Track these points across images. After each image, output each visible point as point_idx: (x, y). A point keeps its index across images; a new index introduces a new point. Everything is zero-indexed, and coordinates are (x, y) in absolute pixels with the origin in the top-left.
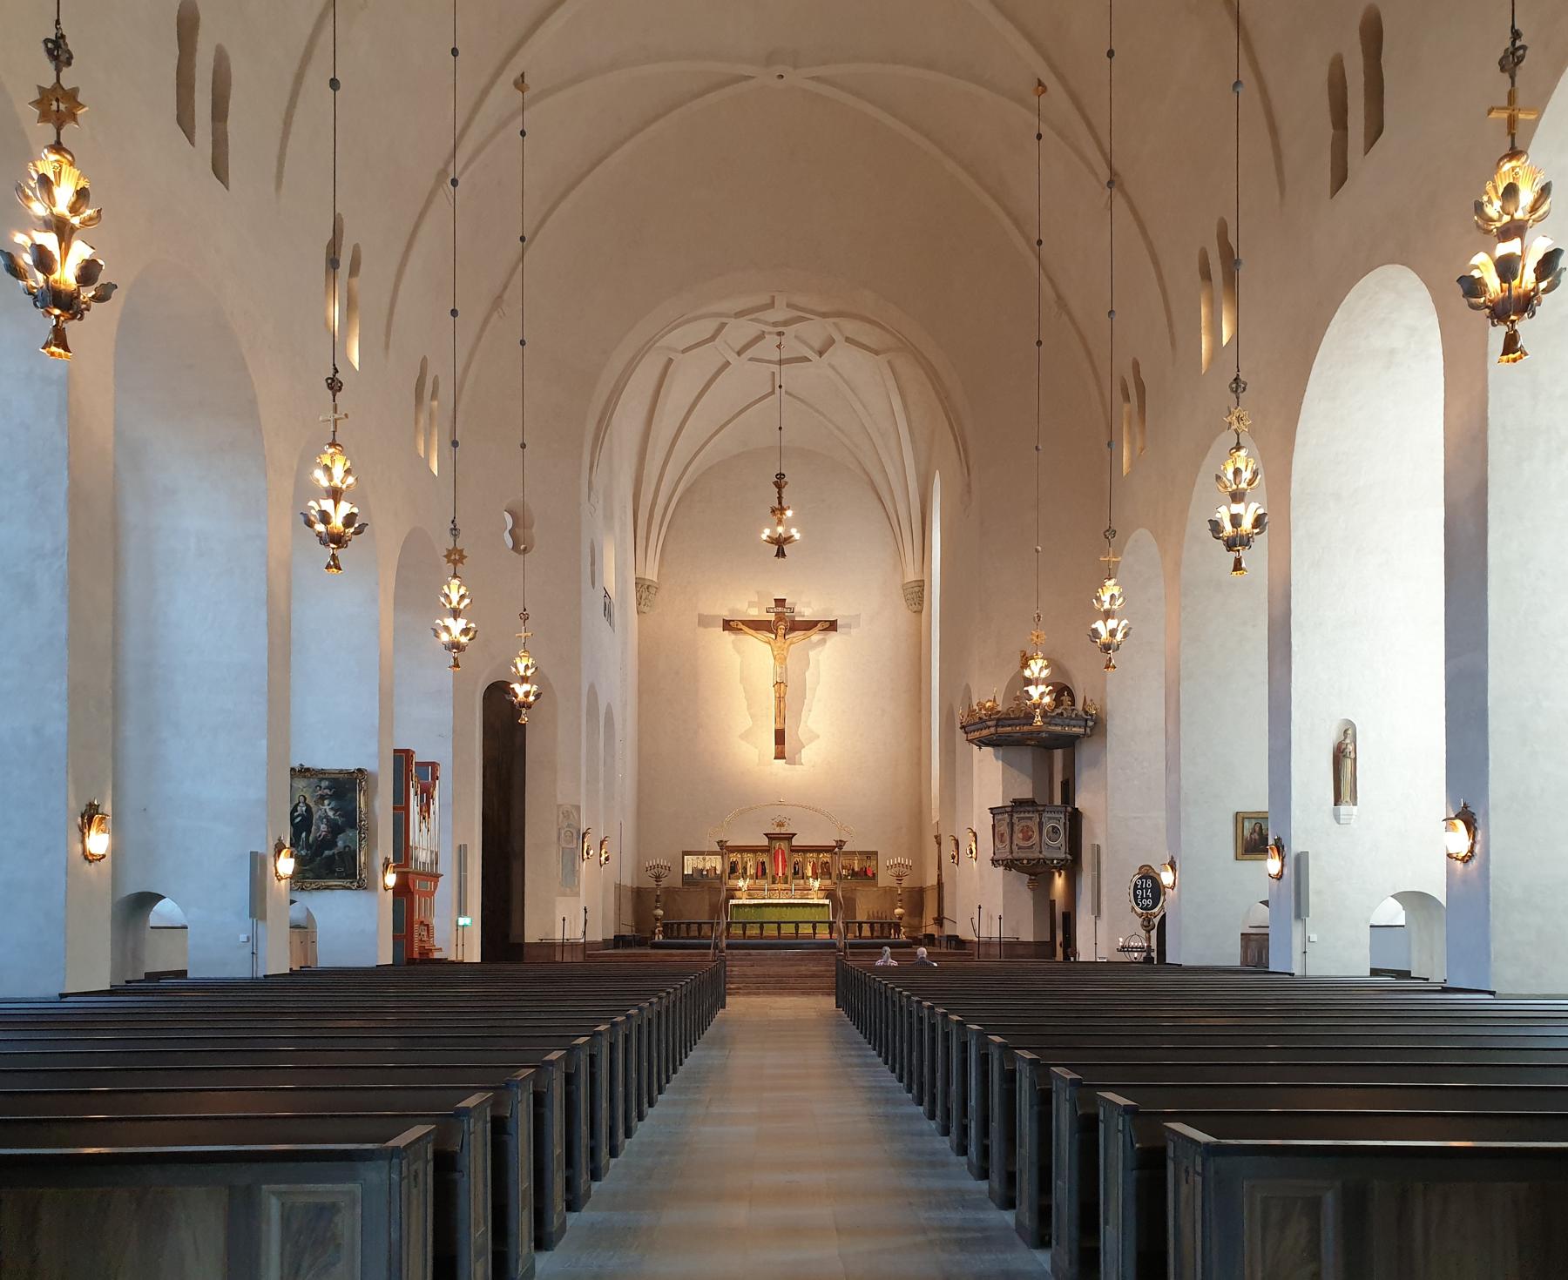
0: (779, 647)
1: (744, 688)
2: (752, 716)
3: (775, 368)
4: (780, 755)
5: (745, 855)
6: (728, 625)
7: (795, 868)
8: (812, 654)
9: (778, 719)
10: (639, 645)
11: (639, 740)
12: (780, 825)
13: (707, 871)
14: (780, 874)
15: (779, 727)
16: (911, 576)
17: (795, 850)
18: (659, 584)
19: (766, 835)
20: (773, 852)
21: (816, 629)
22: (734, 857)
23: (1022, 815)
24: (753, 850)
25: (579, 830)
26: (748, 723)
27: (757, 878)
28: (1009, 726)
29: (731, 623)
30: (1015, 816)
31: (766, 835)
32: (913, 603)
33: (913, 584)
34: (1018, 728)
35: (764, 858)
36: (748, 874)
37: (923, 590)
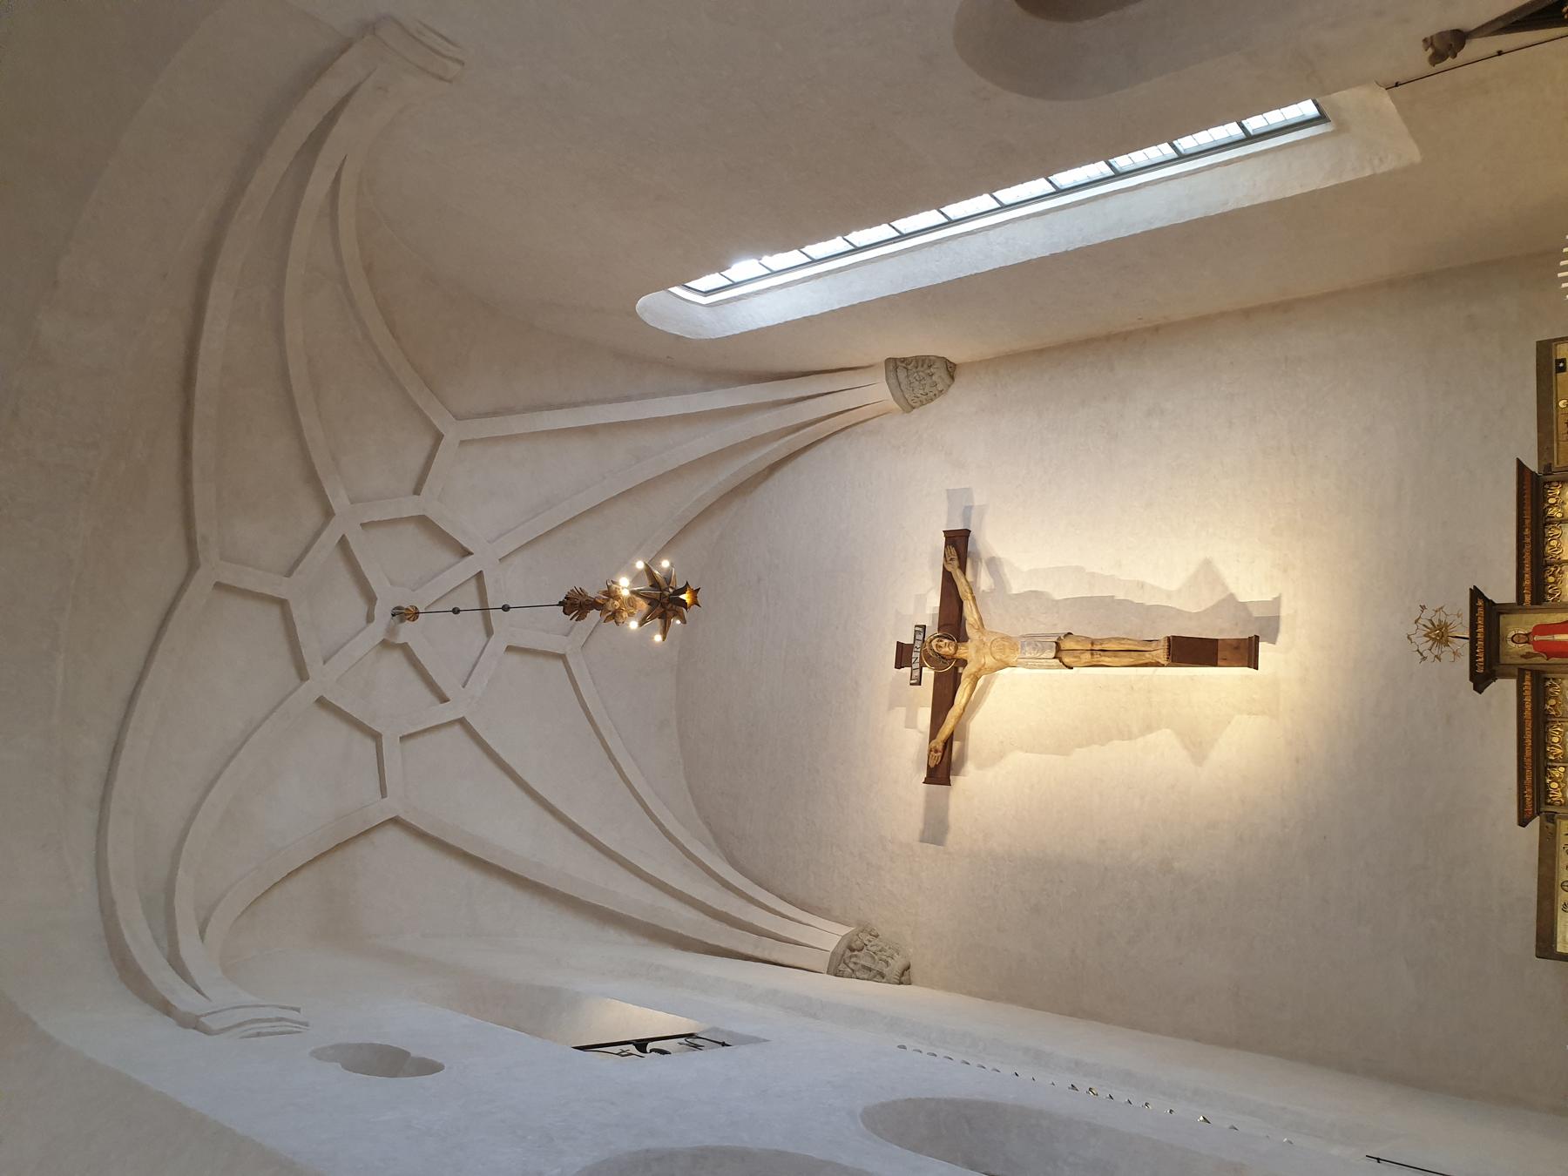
0: (978, 650)
1: (1080, 746)
2: (1148, 728)
4: (1246, 653)
6: (941, 770)
8: (1016, 586)
9: (1148, 657)
10: (970, 993)
11: (1197, 1040)
12: (1440, 635)
15: (1161, 654)
16: (878, 391)
18: (859, 925)
20: (1541, 660)
21: (957, 574)
26: (1164, 739)
29: (932, 765)
32: (928, 381)
33: (893, 381)
37: (904, 360)
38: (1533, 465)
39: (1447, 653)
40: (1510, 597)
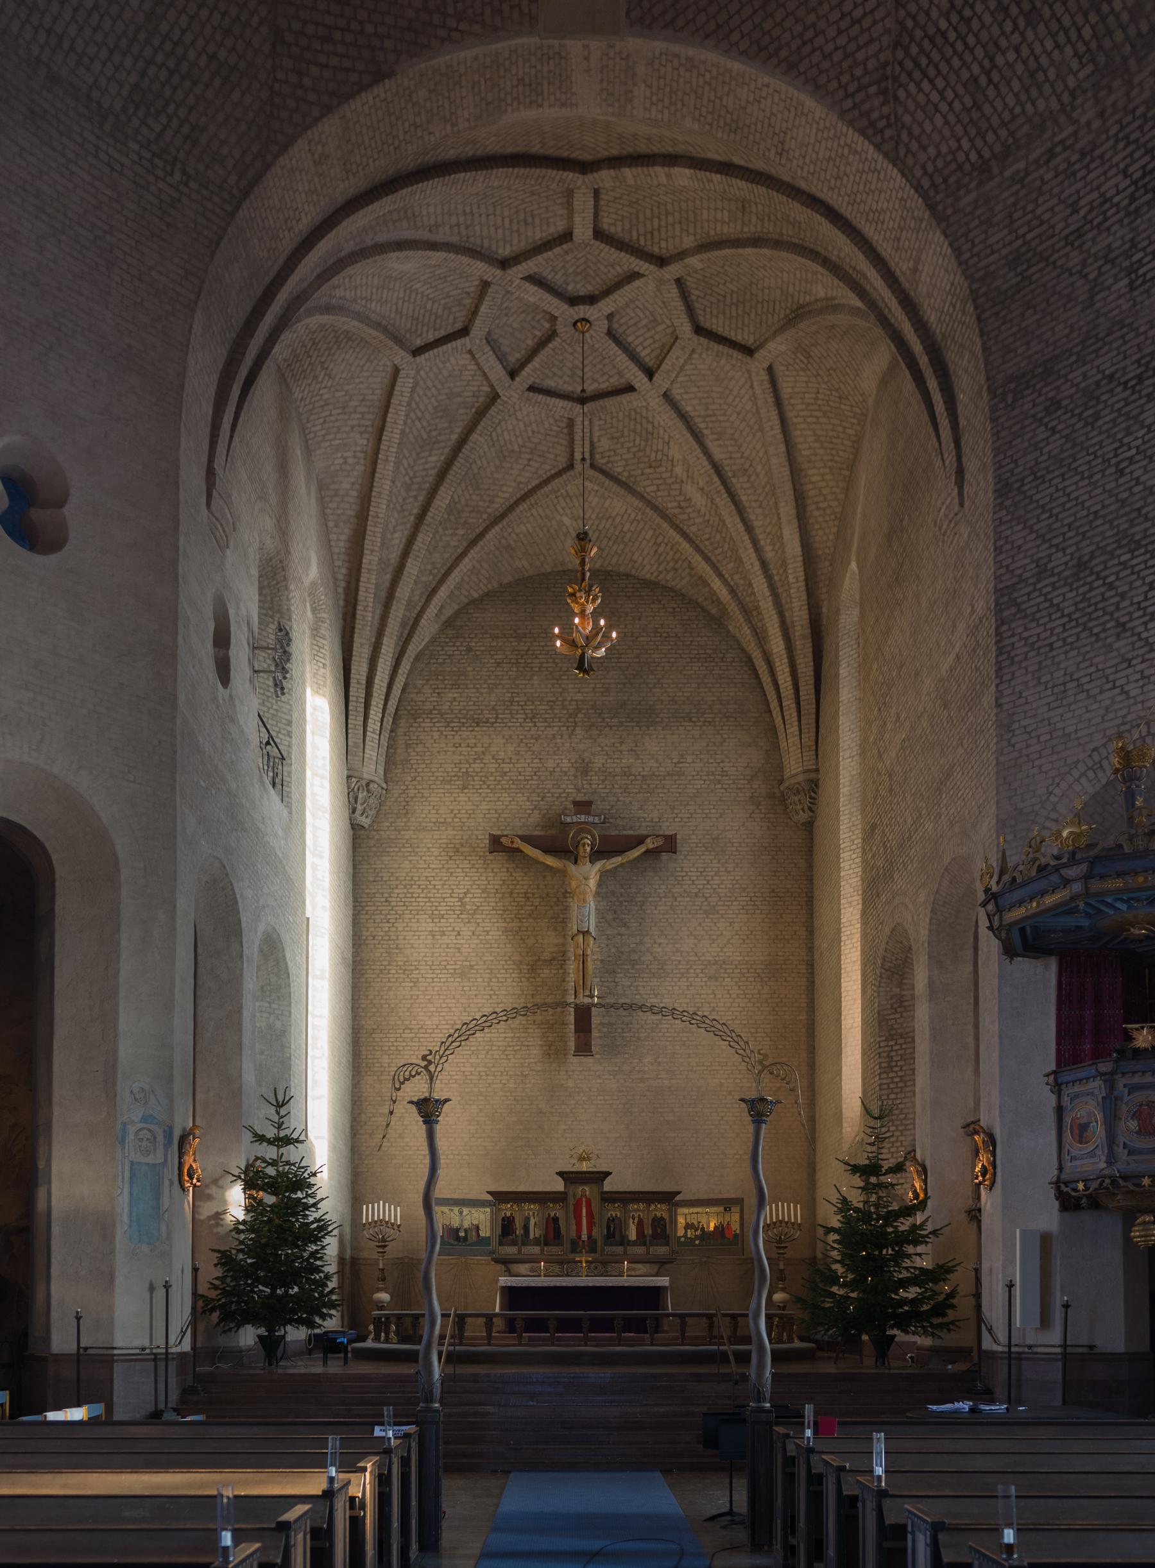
3: (578, 408)
5: (526, 1206)
7: (608, 1228)
13: (466, 1231)
14: (584, 1237)
17: (610, 1198)
19: (560, 1174)
22: (507, 1209)
23: (1137, 1079)
24: (541, 1198)
25: (171, 1128)
27: (546, 1244)
28: (1119, 875)
30: (1121, 1082)
31: (560, 1174)
34: (1141, 879)
35: (556, 1211)
36: (532, 1236)
38: (678, 1198)
39: (574, 1161)
40: (606, 1189)
